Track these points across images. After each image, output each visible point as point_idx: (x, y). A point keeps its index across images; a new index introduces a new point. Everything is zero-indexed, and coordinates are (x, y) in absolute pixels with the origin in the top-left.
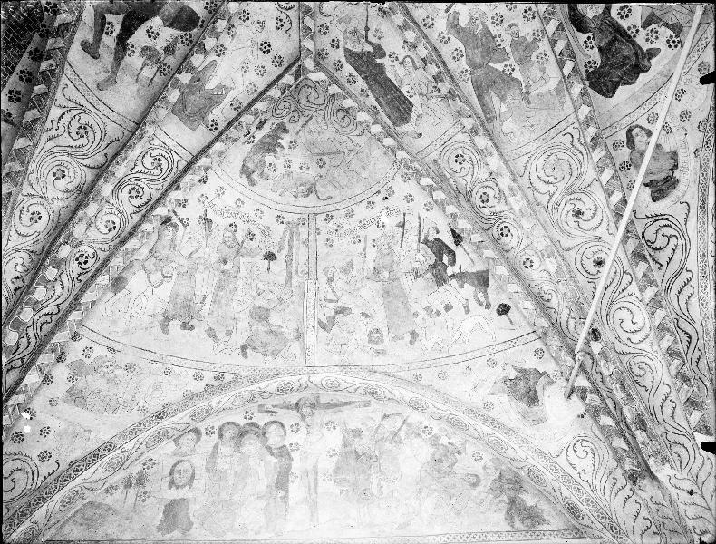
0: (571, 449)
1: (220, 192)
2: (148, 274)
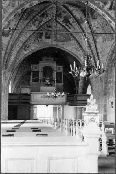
1: (95, 24)
2: (98, 38)
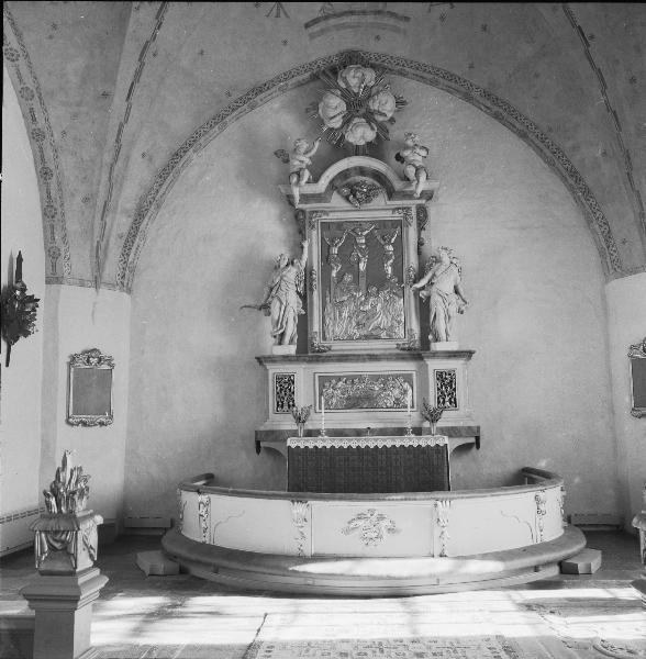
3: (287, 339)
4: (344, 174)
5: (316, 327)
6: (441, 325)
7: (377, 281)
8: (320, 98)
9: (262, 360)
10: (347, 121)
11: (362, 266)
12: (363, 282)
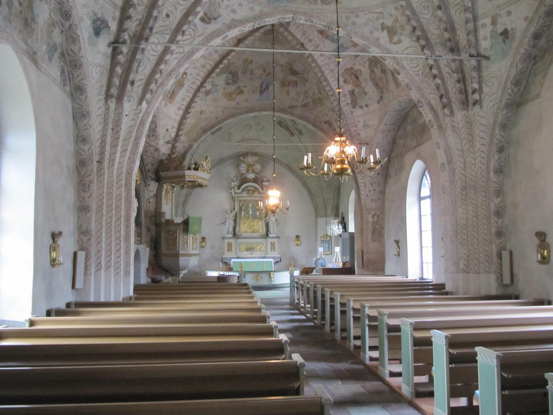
0: (95, 66)
3: (230, 232)
4: (247, 187)
5: (237, 229)
6: (271, 230)
7: (255, 217)
8: (239, 164)
9: (223, 238)
10: (248, 171)
11: (250, 213)
12: (251, 217)
